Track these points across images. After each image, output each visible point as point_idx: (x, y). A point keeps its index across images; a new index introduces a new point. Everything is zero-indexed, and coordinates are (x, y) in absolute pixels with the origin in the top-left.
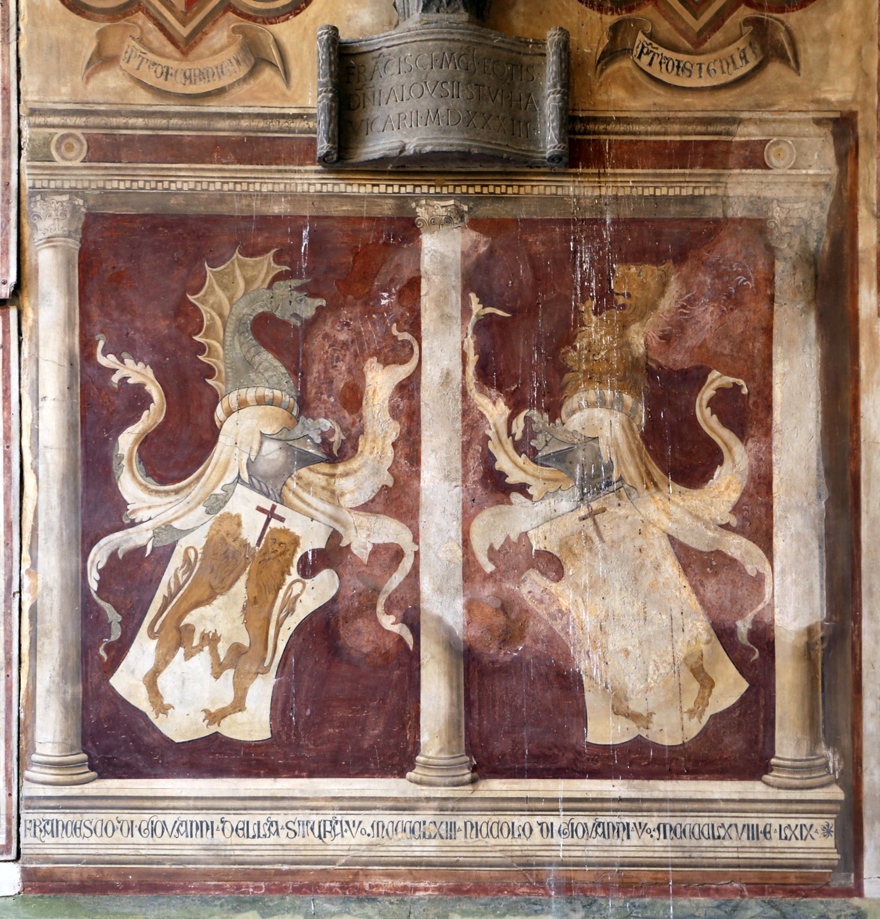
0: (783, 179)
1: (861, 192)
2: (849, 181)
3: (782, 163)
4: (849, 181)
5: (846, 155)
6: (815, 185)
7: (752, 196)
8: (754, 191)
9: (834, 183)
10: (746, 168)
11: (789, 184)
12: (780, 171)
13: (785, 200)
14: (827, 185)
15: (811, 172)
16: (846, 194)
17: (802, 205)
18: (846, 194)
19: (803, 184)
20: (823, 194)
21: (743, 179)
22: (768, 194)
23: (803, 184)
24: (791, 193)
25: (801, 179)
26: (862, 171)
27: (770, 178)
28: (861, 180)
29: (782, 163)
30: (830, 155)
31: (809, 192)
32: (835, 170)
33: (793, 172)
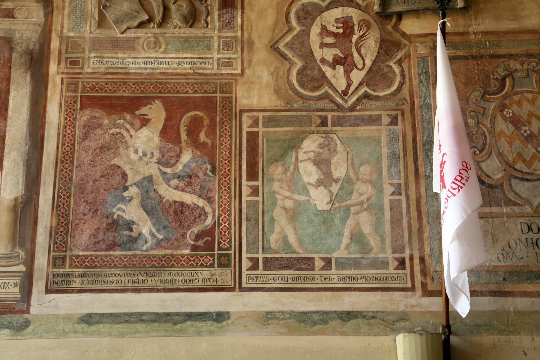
0: (21, 22)
1: (53, 27)
2: (49, 23)
3: (21, 16)
4: (49, 23)
5: (48, 14)
6: (34, 25)
7: (7, 28)
8: (8, 27)
9: (43, 24)
10: (5, 18)
11: (23, 24)
12: (19, 19)
13: (21, 30)
14: (39, 25)
15: (33, 20)
16: (47, 28)
17: (28, 32)
18: (47, 28)
19: (29, 24)
20: (38, 28)
21: (4, 22)
22: (14, 28)
23: (29, 24)
24: (24, 27)
25: (29, 23)
26: (55, 20)
27: (15, 22)
28: (54, 23)
29: (21, 16)
30: (42, 14)
31: (32, 27)
32: (43, 19)
33: (26, 20)
